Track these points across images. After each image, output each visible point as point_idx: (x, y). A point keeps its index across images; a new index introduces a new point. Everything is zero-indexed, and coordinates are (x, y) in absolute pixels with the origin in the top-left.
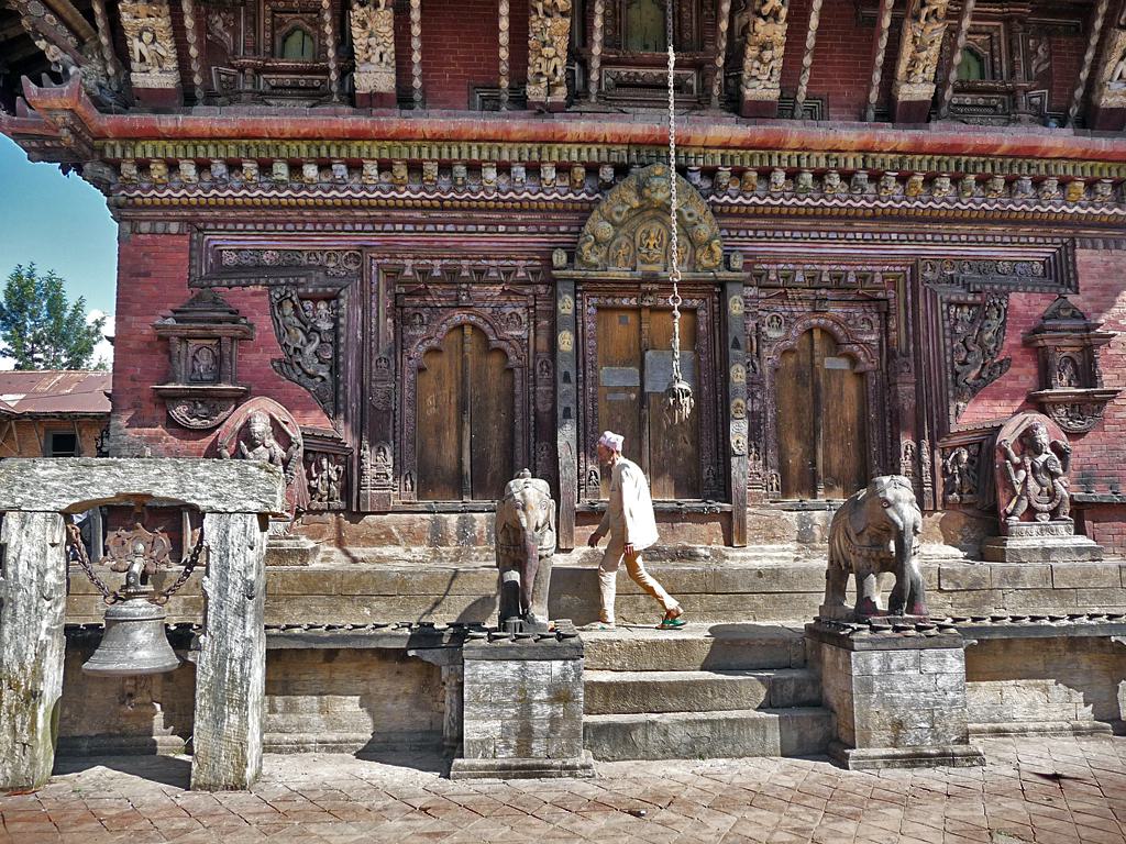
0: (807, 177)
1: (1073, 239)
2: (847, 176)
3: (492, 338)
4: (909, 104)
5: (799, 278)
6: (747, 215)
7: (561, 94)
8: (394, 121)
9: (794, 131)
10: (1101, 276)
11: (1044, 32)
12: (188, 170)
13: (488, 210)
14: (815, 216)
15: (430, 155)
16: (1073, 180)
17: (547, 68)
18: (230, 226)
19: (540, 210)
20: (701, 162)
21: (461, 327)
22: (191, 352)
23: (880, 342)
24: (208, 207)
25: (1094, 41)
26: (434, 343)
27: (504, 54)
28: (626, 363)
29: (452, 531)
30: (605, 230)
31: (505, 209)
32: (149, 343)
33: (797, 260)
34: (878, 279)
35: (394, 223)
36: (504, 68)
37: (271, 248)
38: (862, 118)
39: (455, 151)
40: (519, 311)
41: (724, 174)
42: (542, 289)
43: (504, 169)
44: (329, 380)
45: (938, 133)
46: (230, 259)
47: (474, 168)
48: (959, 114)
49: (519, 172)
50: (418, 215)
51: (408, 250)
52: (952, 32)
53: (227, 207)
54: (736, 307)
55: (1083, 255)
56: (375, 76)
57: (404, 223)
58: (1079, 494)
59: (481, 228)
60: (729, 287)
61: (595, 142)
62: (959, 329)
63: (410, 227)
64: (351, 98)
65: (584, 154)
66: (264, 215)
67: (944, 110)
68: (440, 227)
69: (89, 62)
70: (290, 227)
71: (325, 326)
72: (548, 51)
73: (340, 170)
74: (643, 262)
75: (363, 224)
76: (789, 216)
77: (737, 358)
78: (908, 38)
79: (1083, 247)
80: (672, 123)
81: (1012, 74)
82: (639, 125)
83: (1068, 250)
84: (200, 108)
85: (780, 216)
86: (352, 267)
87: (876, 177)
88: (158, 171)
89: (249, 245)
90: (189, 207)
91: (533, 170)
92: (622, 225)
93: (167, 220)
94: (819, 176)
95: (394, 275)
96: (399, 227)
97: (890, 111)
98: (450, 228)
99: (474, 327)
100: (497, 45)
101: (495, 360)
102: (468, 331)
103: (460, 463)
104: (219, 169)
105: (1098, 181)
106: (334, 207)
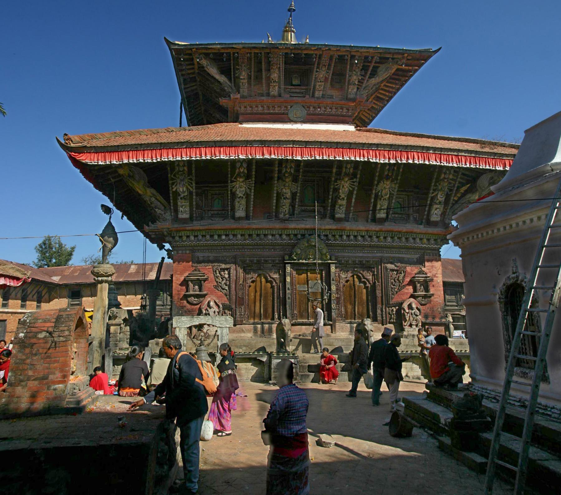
0: (352, 237)
2: (363, 236)
4: (379, 218)
5: (350, 262)
8: (245, 224)
9: (348, 226)
12: (192, 238)
14: (354, 246)
24: (197, 246)
28: (304, 284)
33: (349, 257)
34: (371, 262)
41: (330, 236)
43: (273, 235)
46: (201, 259)
47: (265, 235)
49: (277, 236)
50: (251, 247)
53: (201, 246)
56: (240, 213)
58: (424, 320)
64: (233, 217)
67: (389, 220)
72: (284, 207)
80: (316, 223)
82: (307, 224)
84: (195, 222)
85: (345, 246)
86: (233, 260)
87: (370, 237)
88: (185, 238)
89: (206, 255)
90: (192, 246)
93: (186, 250)
94: (355, 237)
97: (374, 220)
104: (200, 237)
106: (229, 245)
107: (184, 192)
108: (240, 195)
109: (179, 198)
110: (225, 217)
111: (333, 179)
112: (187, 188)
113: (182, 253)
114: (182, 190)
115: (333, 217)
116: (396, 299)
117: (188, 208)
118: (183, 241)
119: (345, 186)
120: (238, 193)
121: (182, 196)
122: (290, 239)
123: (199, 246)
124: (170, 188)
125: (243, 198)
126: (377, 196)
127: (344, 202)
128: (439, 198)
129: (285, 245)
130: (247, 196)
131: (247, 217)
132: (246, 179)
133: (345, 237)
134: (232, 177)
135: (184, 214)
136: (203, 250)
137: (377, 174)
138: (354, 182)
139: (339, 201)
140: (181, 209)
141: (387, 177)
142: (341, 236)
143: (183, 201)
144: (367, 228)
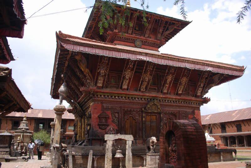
2: (173, 101)
8: (127, 92)
9: (168, 96)
12: (102, 96)
21: (130, 117)
30: (149, 106)
33: (168, 110)
37: (110, 106)
38: (174, 94)
42: (140, 112)
43: (138, 98)
47: (135, 98)
48: (184, 94)
52: (184, 87)
53: (106, 101)
54: (162, 116)
55: (195, 111)
56: (125, 87)
66: (110, 102)
73: (120, 97)
81: (188, 90)
83: (194, 110)
84: (104, 89)
90: (101, 100)
91: (141, 99)
93: (99, 102)
97: (177, 94)
99: (132, 117)
100: (139, 84)
101: (134, 121)
102: (131, 117)
104: (106, 96)
107: (103, 73)
108: (127, 78)
110: (117, 88)
112: (104, 71)
113: (97, 103)
115: (162, 92)
117: (103, 81)
119: (169, 78)
120: (126, 77)
121: (102, 75)
122: (145, 101)
124: (97, 70)
125: (127, 79)
126: (180, 83)
130: (130, 79)
132: (131, 71)
133: (167, 101)
134: (125, 69)
138: (173, 77)
140: (99, 81)
142: (165, 101)
143: (101, 77)
144: (176, 98)
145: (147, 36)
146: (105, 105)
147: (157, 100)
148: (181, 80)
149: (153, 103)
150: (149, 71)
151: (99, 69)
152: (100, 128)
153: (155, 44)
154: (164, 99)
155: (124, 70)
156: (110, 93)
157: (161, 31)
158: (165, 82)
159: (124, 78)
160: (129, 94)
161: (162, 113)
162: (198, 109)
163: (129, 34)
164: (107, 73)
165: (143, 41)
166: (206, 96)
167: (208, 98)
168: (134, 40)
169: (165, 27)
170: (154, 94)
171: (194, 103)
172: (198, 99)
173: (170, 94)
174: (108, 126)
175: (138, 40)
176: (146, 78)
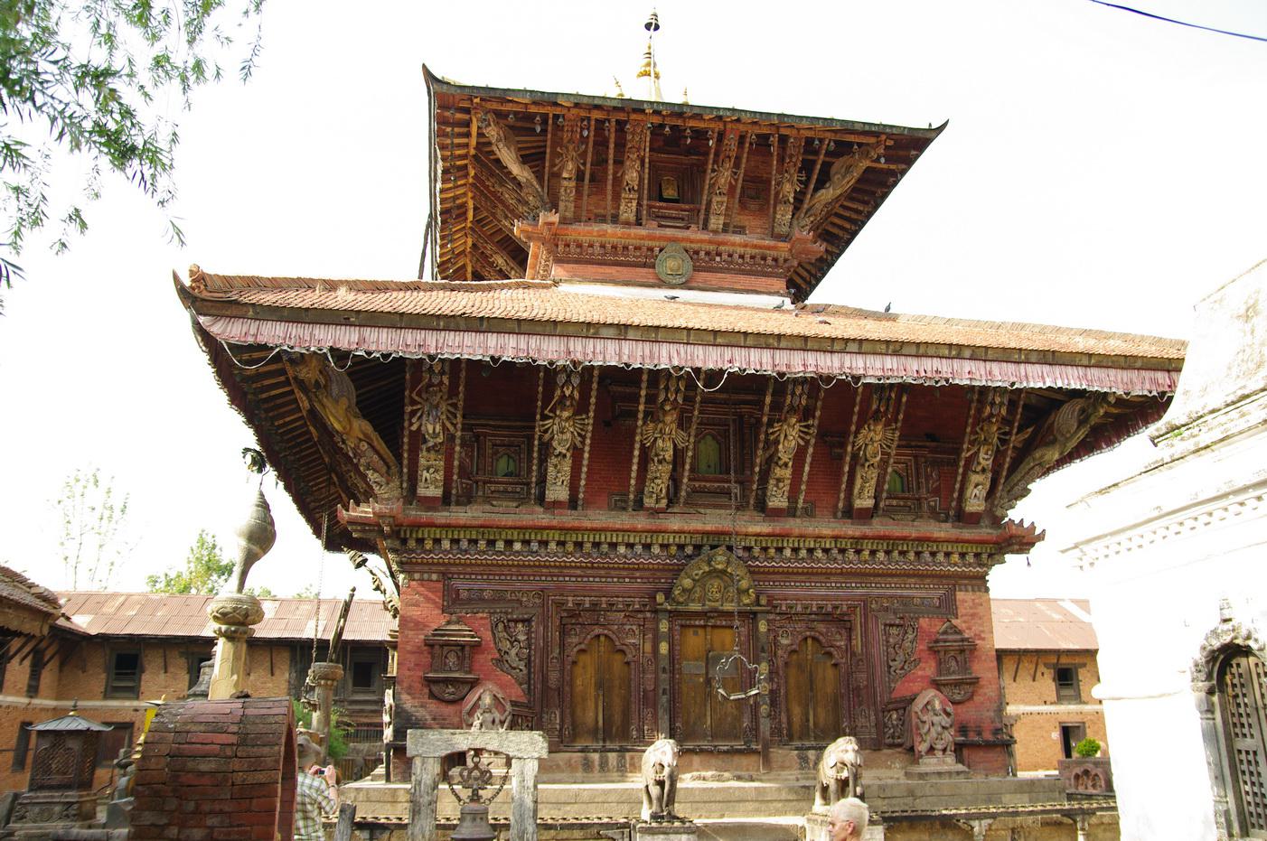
1: (954, 585)
2: (826, 551)
3: (617, 643)
6: (768, 573)
7: (664, 503)
8: (568, 518)
9: (794, 525)
10: (971, 608)
11: (935, 463)
13: (619, 569)
14: (807, 573)
15: (588, 539)
16: (952, 553)
17: (657, 489)
18: (467, 576)
19: (649, 569)
20: (743, 544)
21: (598, 636)
22: (445, 653)
23: (846, 646)
25: (959, 478)
26: (583, 646)
27: (633, 482)
29: (597, 763)
31: (628, 569)
32: (419, 647)
35: (564, 576)
36: (632, 489)
37: (488, 588)
38: (835, 516)
39: (603, 537)
40: (634, 628)
42: (648, 615)
43: (630, 546)
44: (525, 671)
45: (878, 527)
47: (613, 546)
48: (890, 512)
51: (571, 591)
54: (763, 627)
55: (960, 595)
57: (570, 576)
59: (615, 580)
60: (759, 615)
61: (684, 533)
62: (891, 640)
63: (574, 579)
65: (677, 540)
66: (488, 569)
67: (880, 512)
68: (591, 579)
69: (393, 482)
70: (503, 577)
71: (522, 638)
72: (659, 481)
73: (535, 546)
74: (710, 600)
75: (546, 576)
76: (793, 573)
77: (764, 658)
78: (859, 476)
79: (960, 590)
84: (453, 508)
86: (537, 601)
87: (843, 551)
88: (429, 545)
90: (444, 564)
91: (647, 547)
92: (698, 580)
95: (560, 605)
96: (567, 579)
97: (850, 513)
98: (597, 579)
99: (606, 636)
101: (618, 657)
103: (597, 722)
104: (464, 545)
105: (966, 553)
107: (435, 435)
108: (559, 449)
109: (424, 447)
110: (522, 500)
111: (765, 419)
112: (443, 425)
114: (431, 431)
115: (761, 506)
116: (902, 689)
117: (442, 473)
118: (425, 552)
119: (790, 437)
120: (555, 444)
121: (431, 444)
122: (671, 557)
123: (460, 564)
124: (406, 424)
125: (565, 456)
126: (855, 457)
127: (787, 473)
128: (981, 460)
129: (658, 570)
130: (577, 453)
131: (573, 503)
132: (575, 414)
133: (788, 553)
134: (544, 408)
135: (430, 487)
136: (471, 574)
137: (857, 409)
138: (807, 427)
139: (778, 470)
140: (425, 474)
141: (876, 416)
142: (780, 550)
143: (433, 455)
144: (836, 532)
145: (716, 222)
146: (457, 583)
147: (730, 548)
148: (861, 442)
149: (710, 565)
150: (667, 408)
151: (414, 420)
152: (432, 695)
153: (764, 258)
154: (772, 544)
155: (539, 410)
156: (481, 527)
157: (789, 190)
158: (771, 461)
159: (546, 449)
160: (576, 530)
161: (762, 612)
162: (980, 582)
163: (627, 224)
164: (459, 434)
165: (697, 253)
166: (1021, 512)
167: (1026, 525)
168: (651, 249)
169: (807, 167)
170: (713, 520)
171: (947, 555)
172: (968, 533)
173: (809, 513)
174: (473, 684)
175: (670, 248)
176: (660, 442)
